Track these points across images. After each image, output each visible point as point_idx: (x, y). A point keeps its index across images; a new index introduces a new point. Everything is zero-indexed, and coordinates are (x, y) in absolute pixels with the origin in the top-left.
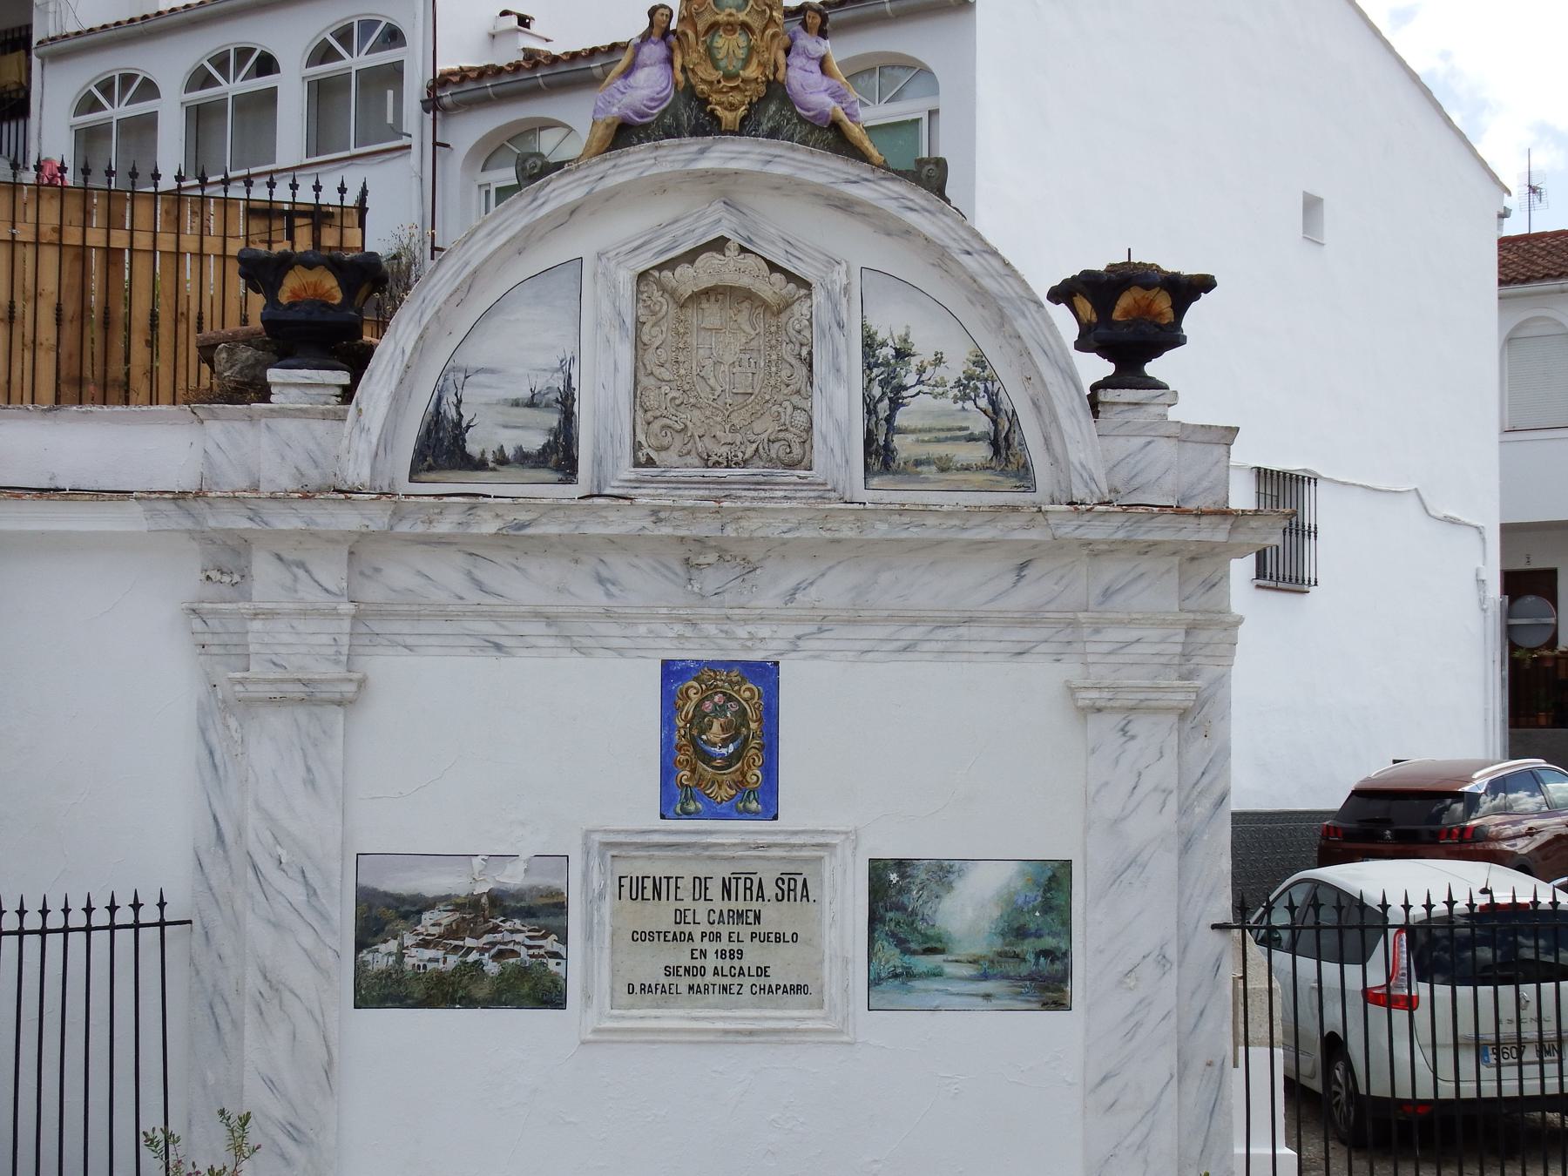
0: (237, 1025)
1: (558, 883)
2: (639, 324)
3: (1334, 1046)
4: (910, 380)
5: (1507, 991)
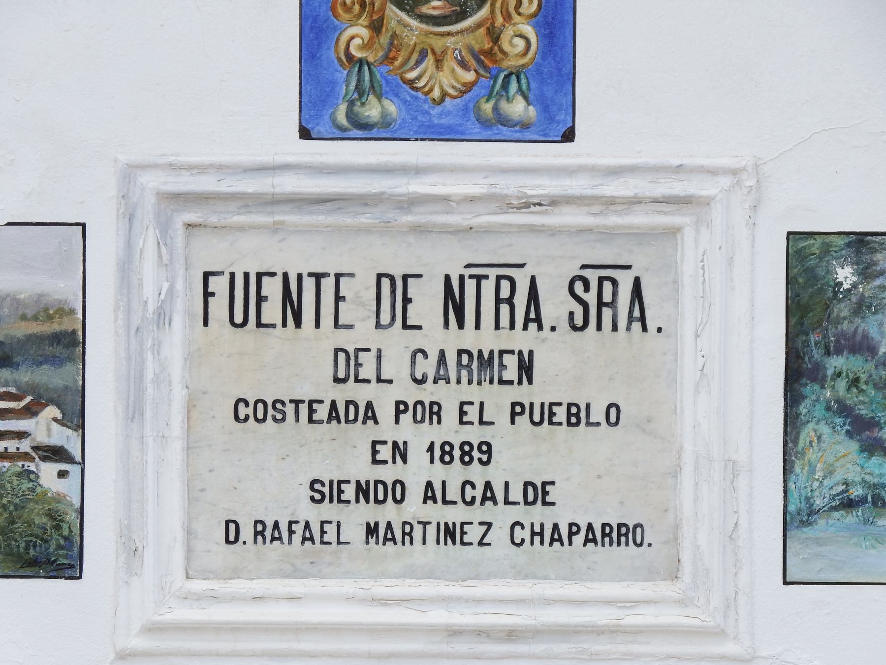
1: (62, 288)
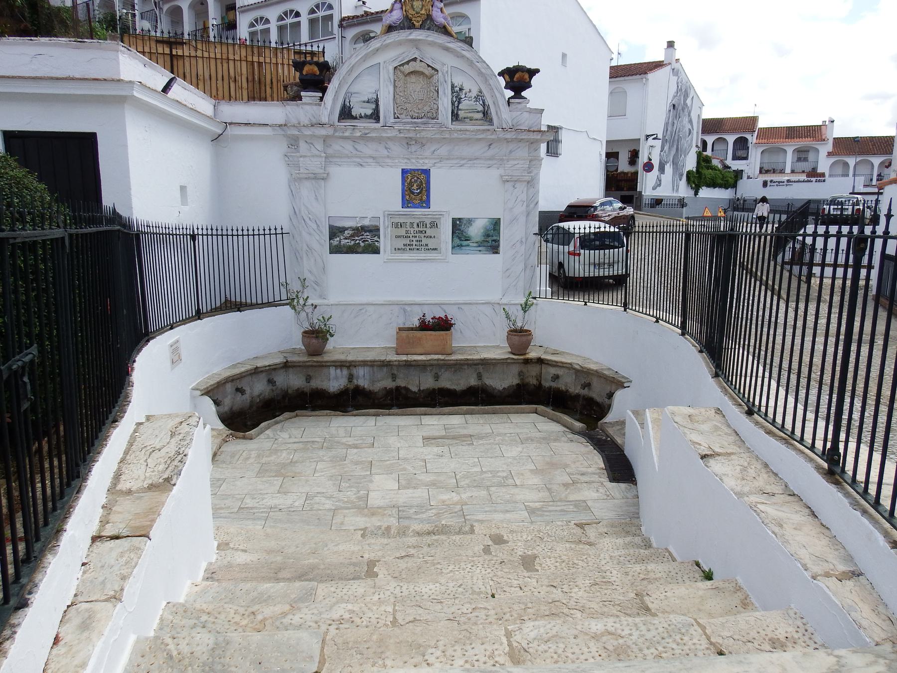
0: (302, 258)
1: (377, 224)
2: (395, 81)
3: (561, 265)
4: (463, 96)
5: (602, 252)
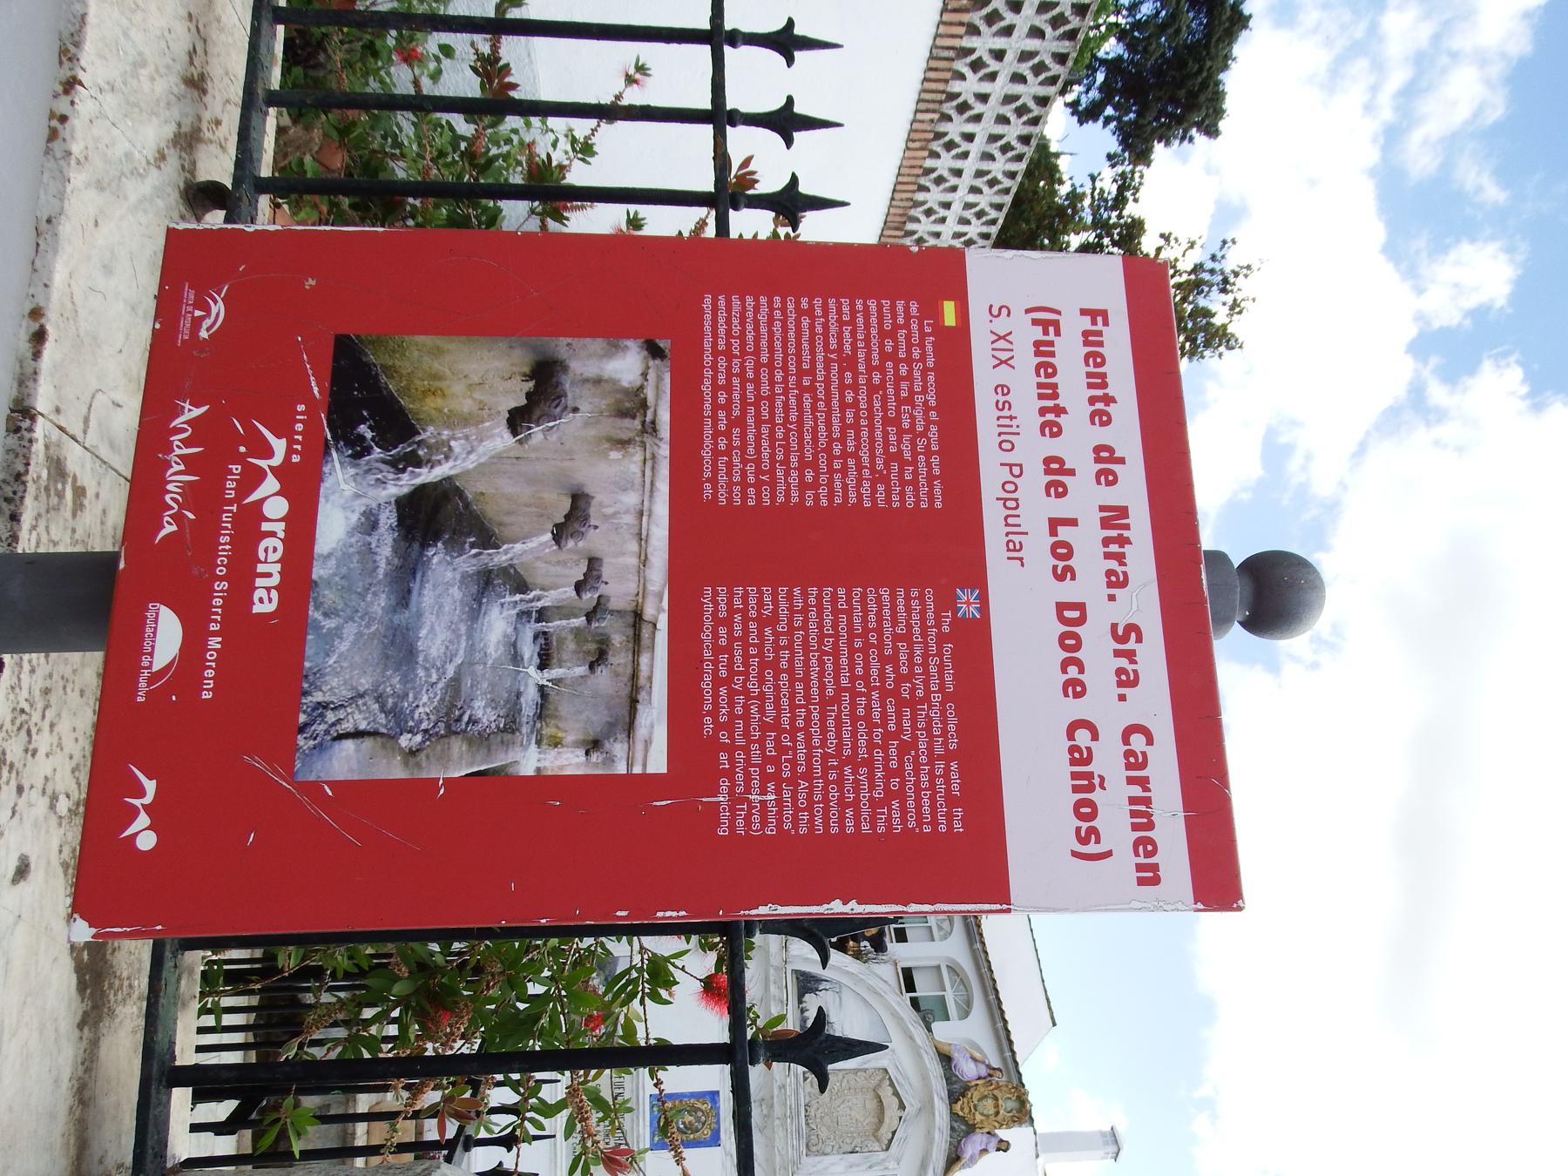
2: (865, 1070)
